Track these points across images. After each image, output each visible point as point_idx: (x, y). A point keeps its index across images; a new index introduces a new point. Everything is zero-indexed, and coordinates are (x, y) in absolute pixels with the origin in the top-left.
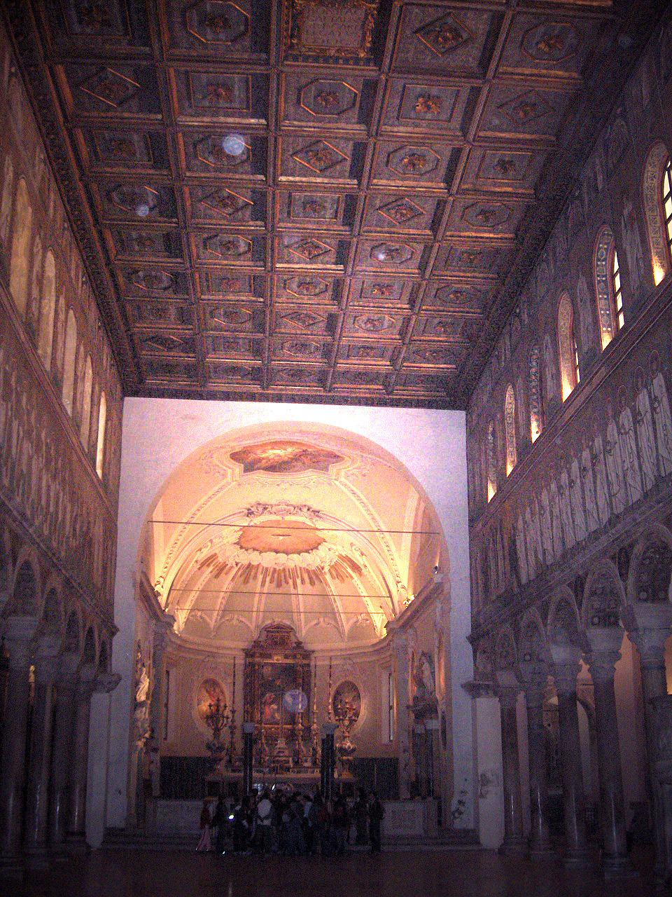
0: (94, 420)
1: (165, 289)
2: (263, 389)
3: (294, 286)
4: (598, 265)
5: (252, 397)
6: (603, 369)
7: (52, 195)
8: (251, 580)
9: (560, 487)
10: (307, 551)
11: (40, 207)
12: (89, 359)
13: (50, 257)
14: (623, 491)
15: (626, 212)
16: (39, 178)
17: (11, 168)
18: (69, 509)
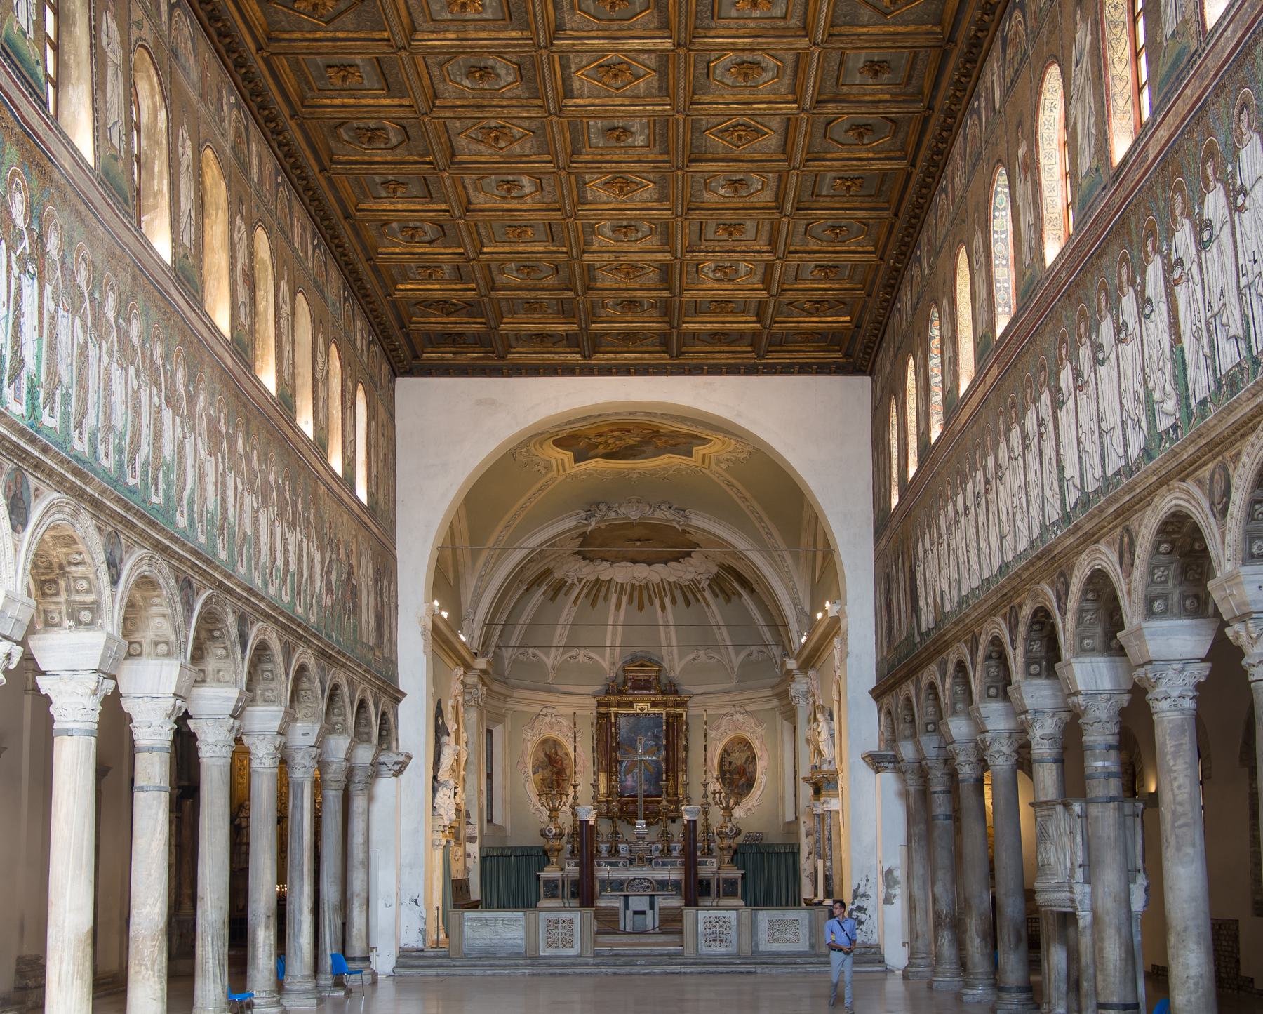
0: (349, 428)
1: (431, 242)
2: (584, 357)
3: (607, 231)
4: (995, 217)
5: (569, 370)
6: (996, 366)
7: (254, 148)
8: (601, 599)
9: (956, 513)
10: (677, 560)
11: (236, 174)
12: (333, 347)
13: (261, 236)
14: (1011, 533)
15: (1021, 153)
16: (232, 132)
17: (188, 143)
18: (318, 558)
